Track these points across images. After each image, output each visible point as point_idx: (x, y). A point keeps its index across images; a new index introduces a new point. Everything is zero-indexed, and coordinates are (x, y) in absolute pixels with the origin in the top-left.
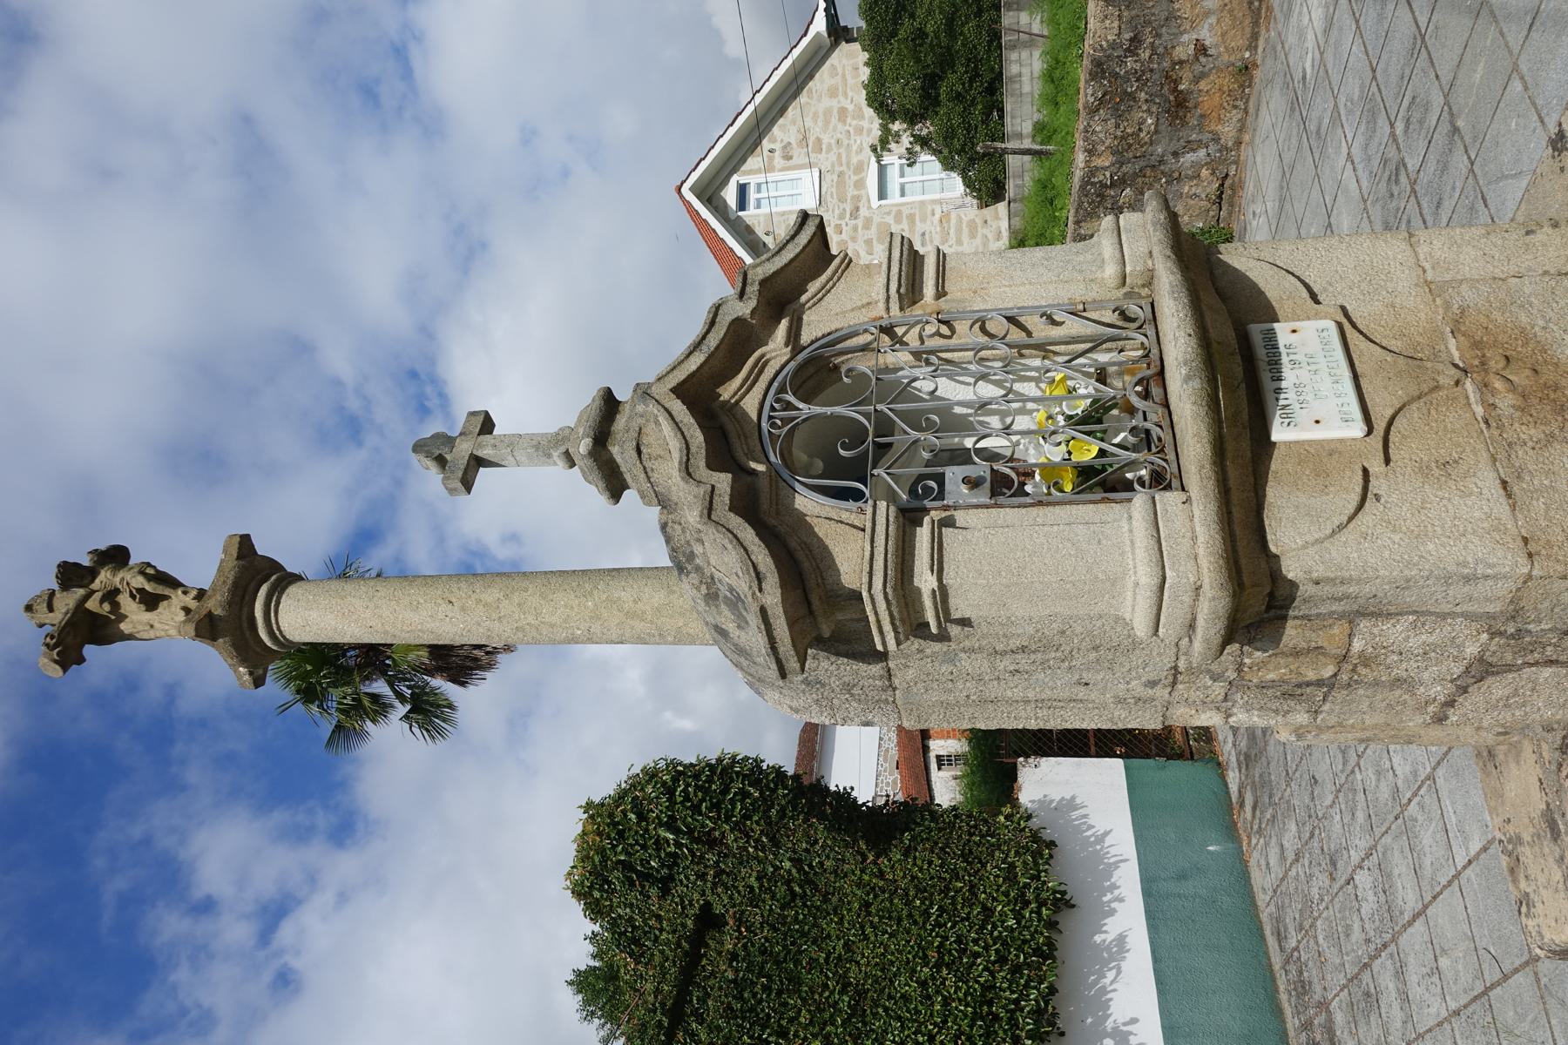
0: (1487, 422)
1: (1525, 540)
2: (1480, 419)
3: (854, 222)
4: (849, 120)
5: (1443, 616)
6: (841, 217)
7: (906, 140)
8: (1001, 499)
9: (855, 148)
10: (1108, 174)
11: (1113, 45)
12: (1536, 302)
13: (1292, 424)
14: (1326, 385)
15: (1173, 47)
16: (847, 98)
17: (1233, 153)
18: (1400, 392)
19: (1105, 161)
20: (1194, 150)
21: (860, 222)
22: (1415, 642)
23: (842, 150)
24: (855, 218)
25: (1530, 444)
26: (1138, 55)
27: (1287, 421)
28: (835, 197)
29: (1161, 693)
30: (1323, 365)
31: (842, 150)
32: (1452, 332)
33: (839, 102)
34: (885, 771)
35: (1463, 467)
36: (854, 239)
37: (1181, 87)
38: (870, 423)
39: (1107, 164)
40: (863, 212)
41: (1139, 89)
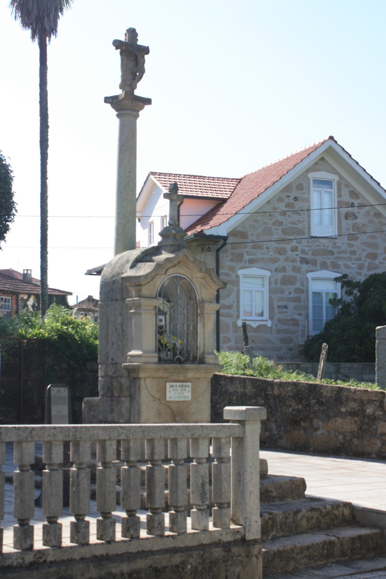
3: (298, 259)
4: (368, 260)
5: (130, 413)
6: (303, 252)
7: (348, 299)
8: (157, 327)
9: (349, 263)
10: (270, 393)
11: (321, 394)
15: (318, 419)
16: (383, 259)
17: (274, 445)
19: (276, 392)
20: (277, 429)
21: (298, 264)
22: (124, 410)
23: (348, 255)
24: (301, 262)
26: (316, 404)
28: (317, 248)
29: (110, 361)
30: (182, 395)
31: (348, 255)
33: (381, 254)
36: (287, 259)
37: (302, 423)
39: (275, 392)
40: (305, 267)
41: (303, 405)
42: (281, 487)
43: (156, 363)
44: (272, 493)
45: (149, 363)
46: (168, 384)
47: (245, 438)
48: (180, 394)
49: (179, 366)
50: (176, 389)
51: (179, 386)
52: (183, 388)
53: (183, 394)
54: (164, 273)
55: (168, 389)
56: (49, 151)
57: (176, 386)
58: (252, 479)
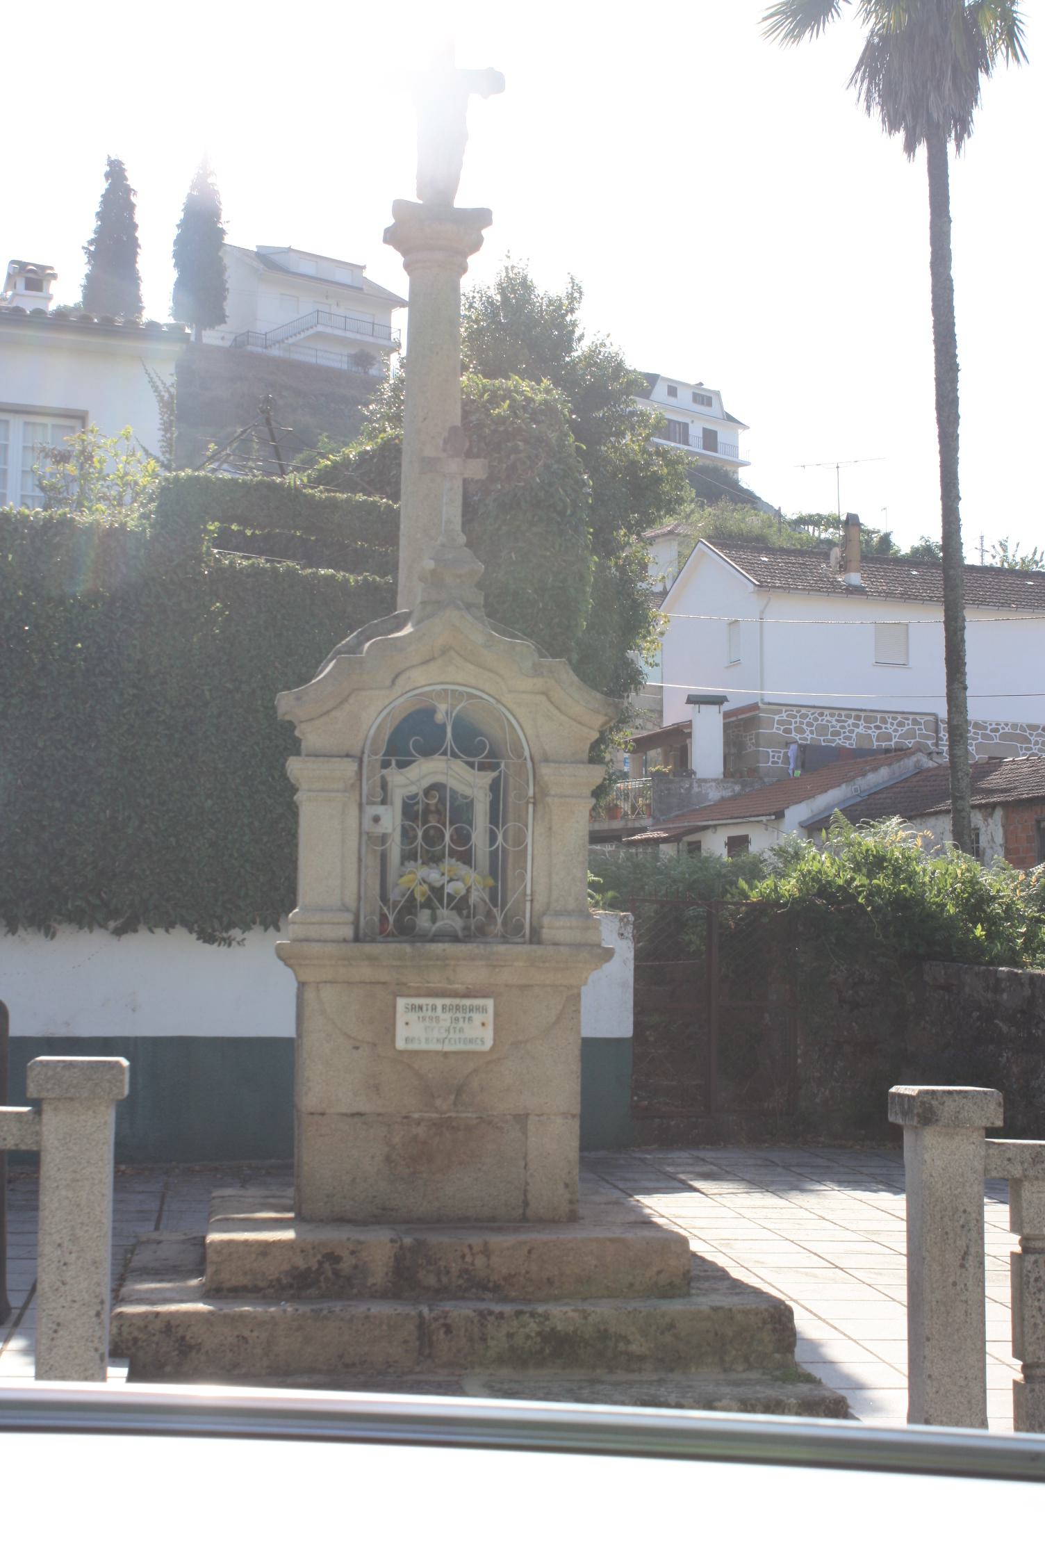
0: (406, 1117)
1: (323, 1114)
8: (364, 838)
27: (410, 1007)
32: (481, 1118)
34: (985, 736)
42: (672, 1326)
43: (345, 941)
44: (628, 1342)
45: (307, 940)
46: (401, 1003)
47: (42, 1154)
48: (448, 1030)
49: (407, 948)
50: (431, 1018)
51: (444, 1007)
52: (459, 1015)
53: (461, 1030)
54: (388, 683)
56: (965, 431)
57: (434, 1008)
58: (64, 1283)
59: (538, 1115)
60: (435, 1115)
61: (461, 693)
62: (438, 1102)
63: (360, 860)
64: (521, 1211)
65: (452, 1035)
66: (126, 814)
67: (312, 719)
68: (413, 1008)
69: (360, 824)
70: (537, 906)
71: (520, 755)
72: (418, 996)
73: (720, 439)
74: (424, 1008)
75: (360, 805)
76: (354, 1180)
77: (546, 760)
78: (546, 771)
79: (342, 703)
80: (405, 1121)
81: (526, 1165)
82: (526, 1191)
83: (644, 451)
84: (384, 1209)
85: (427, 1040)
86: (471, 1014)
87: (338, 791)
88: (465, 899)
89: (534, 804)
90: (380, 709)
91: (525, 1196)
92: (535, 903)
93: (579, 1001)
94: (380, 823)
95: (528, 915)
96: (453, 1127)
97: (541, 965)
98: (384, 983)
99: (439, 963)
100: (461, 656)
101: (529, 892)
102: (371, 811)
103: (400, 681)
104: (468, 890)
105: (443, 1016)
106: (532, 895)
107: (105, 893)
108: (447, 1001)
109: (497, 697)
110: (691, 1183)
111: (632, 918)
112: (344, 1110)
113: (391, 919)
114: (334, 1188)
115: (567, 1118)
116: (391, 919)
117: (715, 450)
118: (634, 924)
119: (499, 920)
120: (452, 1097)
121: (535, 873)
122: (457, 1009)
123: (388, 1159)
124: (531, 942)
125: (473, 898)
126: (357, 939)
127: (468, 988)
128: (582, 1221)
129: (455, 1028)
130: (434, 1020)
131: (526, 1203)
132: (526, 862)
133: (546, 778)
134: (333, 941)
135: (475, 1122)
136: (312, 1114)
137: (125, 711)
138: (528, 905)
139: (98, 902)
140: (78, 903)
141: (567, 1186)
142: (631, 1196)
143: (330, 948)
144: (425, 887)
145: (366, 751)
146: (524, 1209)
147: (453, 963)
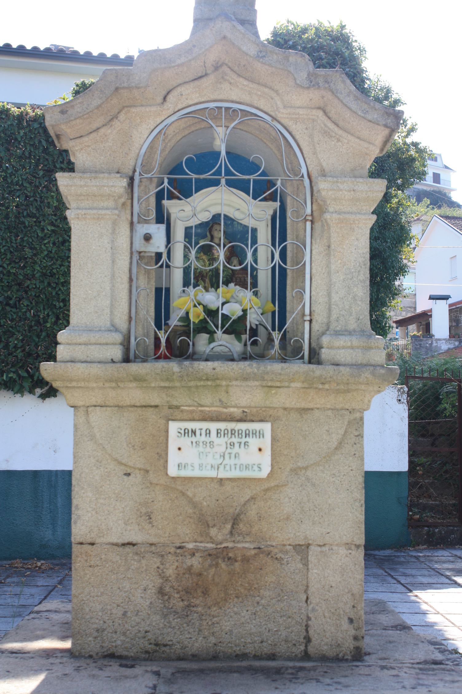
0: (180, 548)
1: (93, 544)
2: (183, 544)
8: (136, 257)
12: (282, 605)
13: (179, 435)
14: (210, 460)
18: (205, 503)
25: (162, 567)
27: (182, 432)
32: (259, 548)
35: (148, 526)
38: (210, 175)
43: (113, 361)
46: (174, 427)
51: (218, 432)
52: (235, 440)
53: (236, 456)
54: (159, 99)
55: (174, 441)
57: (208, 433)
59: (320, 546)
60: (210, 545)
61: (234, 111)
62: (213, 532)
63: (131, 280)
64: (302, 648)
65: (227, 461)
66: (46, 313)
67: (81, 136)
68: (186, 432)
69: (132, 243)
70: (316, 326)
71: (296, 172)
72: (193, 420)
73: (441, 177)
74: (198, 433)
75: (132, 224)
76: (125, 614)
77: (323, 174)
78: (322, 185)
79: (111, 120)
80: (178, 551)
81: (307, 598)
82: (307, 626)
83: (405, 143)
84: (157, 645)
85: (201, 466)
86: (247, 439)
87: (107, 209)
88: (243, 317)
89: (312, 222)
90: (152, 128)
91: (307, 631)
92: (314, 323)
93: (362, 426)
94: (151, 241)
95: (307, 336)
96: (229, 559)
97: (321, 386)
98: (156, 406)
99: (209, 383)
100: (235, 72)
101: (307, 311)
102: (142, 230)
103: (170, 98)
104: (245, 311)
105: (217, 441)
106: (310, 315)
107: (31, 368)
108: (222, 426)
109: (272, 113)
110: (455, 578)
111: (406, 389)
112: (115, 541)
113: (163, 341)
114: (105, 622)
115: (350, 549)
116: (163, 341)
117: (439, 183)
118: (408, 393)
119: (277, 342)
120: (229, 526)
121: (313, 293)
122: (232, 434)
123: (161, 592)
124: (310, 362)
125: (252, 319)
126: (126, 359)
127: (244, 412)
128: (366, 658)
129: (230, 454)
130: (208, 445)
131: (308, 640)
132: (304, 281)
133: (323, 193)
134: (99, 362)
135: (253, 552)
136: (81, 543)
137: (45, 242)
138: (307, 325)
139: (25, 375)
140: (11, 375)
141: (351, 621)
142: (411, 591)
143: (95, 369)
144: (200, 308)
145: (138, 170)
146: (306, 646)
147: (224, 383)
